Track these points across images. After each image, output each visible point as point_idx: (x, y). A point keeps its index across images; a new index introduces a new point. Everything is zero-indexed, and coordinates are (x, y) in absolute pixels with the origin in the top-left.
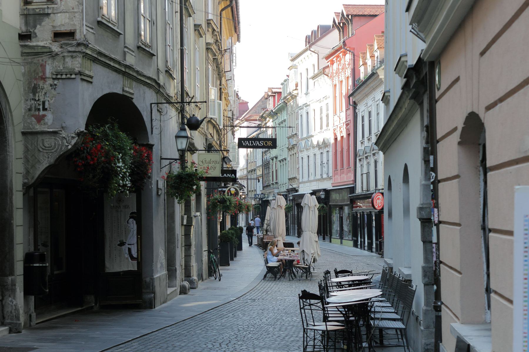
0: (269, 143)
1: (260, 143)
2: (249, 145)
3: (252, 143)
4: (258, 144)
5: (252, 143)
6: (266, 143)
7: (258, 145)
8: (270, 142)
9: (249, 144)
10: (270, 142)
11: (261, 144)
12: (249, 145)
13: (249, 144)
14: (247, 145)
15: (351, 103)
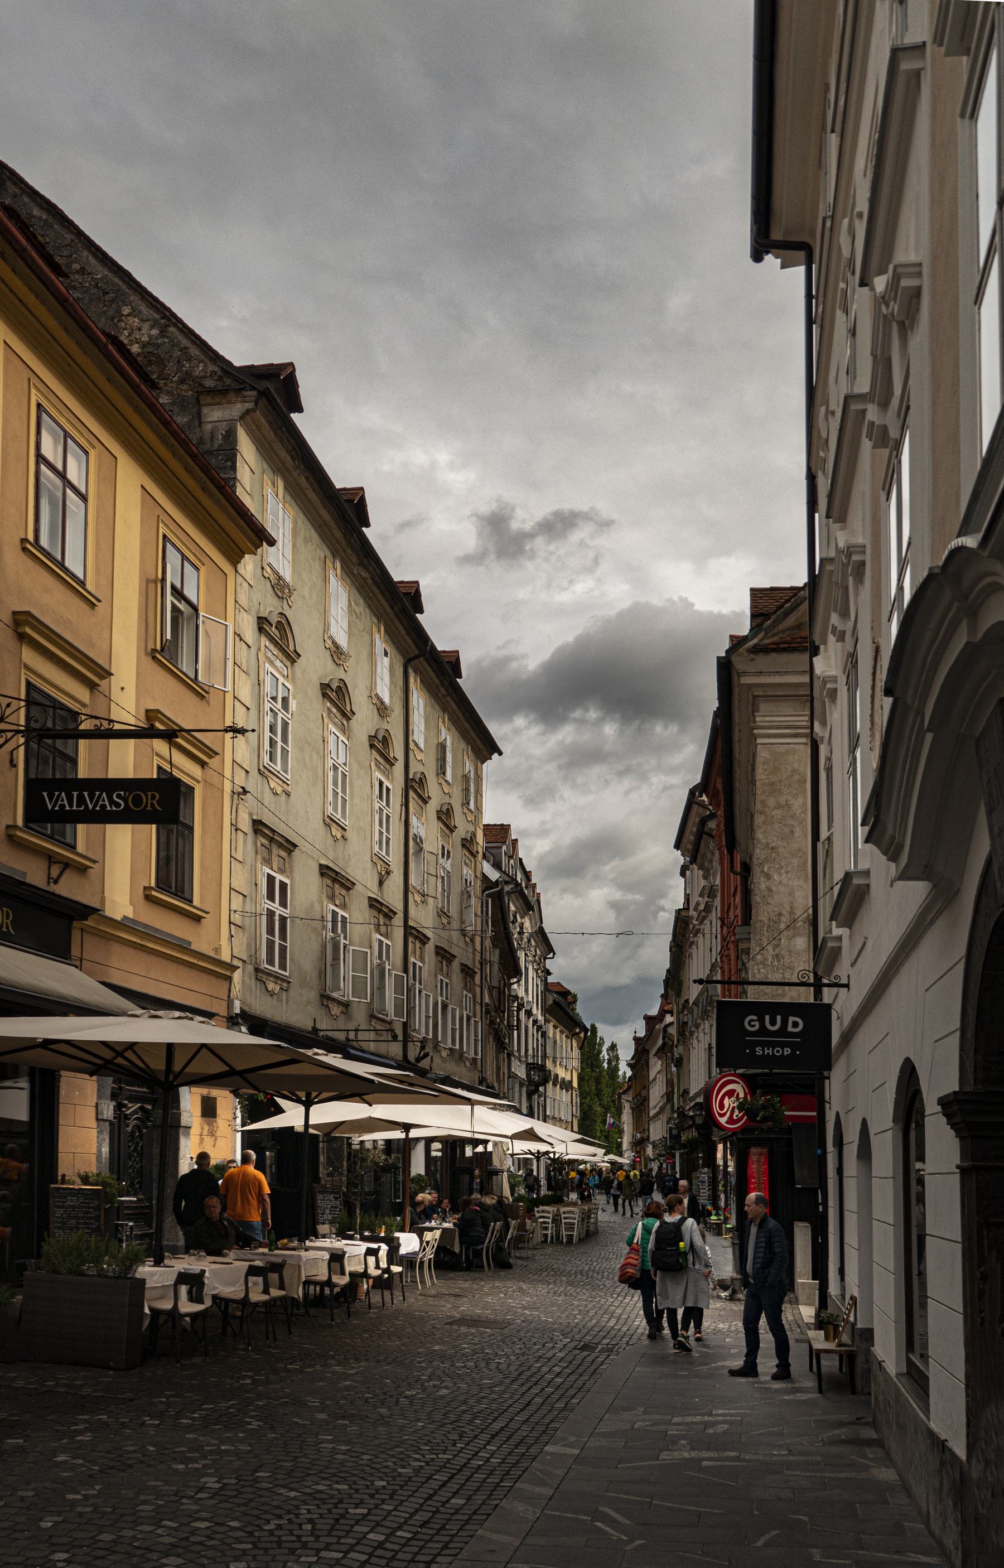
0: (150, 801)
1: (112, 802)
2: (68, 808)
3: (81, 800)
4: (107, 803)
5: (81, 800)
6: (137, 801)
7: (103, 806)
8: (153, 797)
9: (71, 806)
10: (153, 797)
11: (118, 805)
12: (68, 808)
13: (71, 806)
14: (62, 806)
15: (738, 868)
